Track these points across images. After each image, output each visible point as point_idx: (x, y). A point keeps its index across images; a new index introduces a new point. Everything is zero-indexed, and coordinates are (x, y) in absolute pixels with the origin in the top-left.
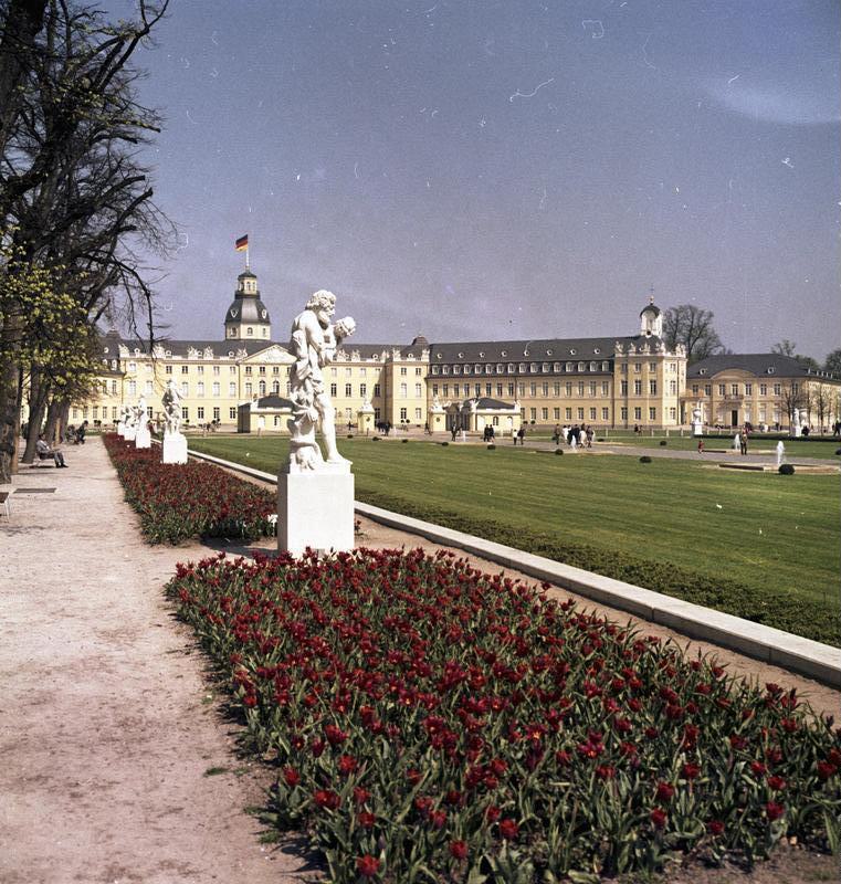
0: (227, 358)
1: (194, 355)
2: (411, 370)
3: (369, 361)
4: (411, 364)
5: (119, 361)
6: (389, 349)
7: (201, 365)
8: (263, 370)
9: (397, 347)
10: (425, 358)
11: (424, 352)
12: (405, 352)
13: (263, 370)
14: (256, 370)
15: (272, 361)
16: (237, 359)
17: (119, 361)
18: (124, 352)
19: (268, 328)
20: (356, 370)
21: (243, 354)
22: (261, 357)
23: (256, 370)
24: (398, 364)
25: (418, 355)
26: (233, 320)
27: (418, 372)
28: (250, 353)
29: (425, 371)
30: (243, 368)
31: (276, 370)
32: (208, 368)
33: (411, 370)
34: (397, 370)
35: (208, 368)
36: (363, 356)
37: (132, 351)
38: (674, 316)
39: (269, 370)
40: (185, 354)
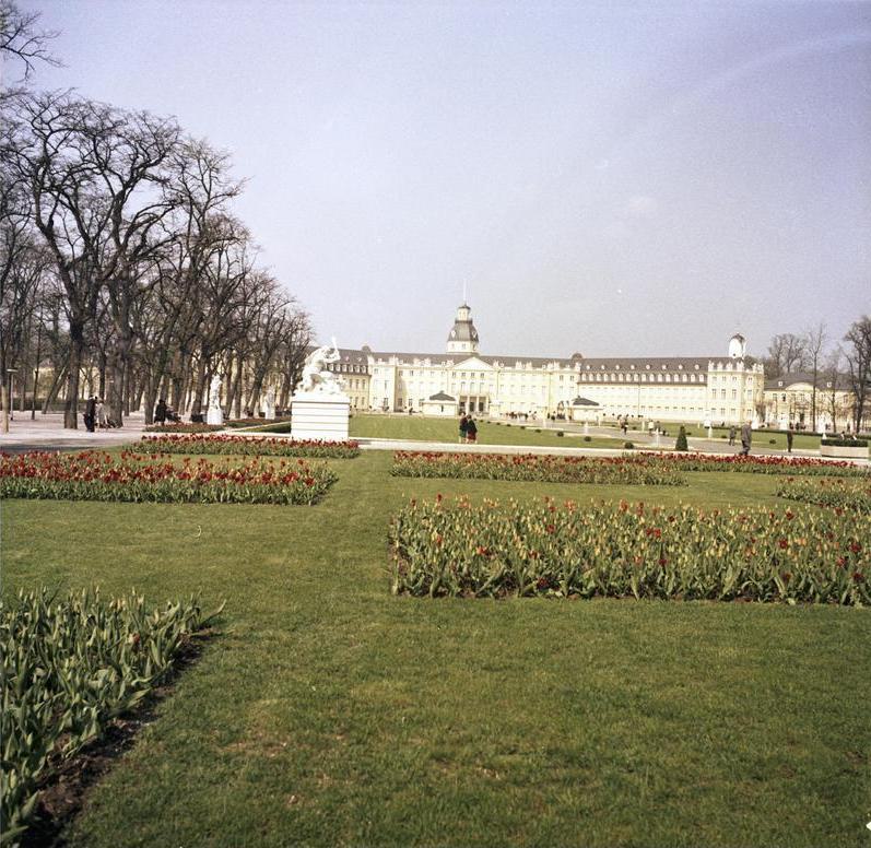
3: (538, 369)
4: (567, 373)
6: (551, 361)
8: (463, 374)
9: (557, 360)
10: (578, 368)
13: (463, 374)
14: (459, 374)
18: (371, 360)
20: (528, 377)
23: (459, 374)
25: (573, 366)
27: (572, 378)
28: (456, 362)
29: (577, 377)
30: (451, 372)
31: (473, 375)
32: (427, 373)
35: (427, 373)
37: (376, 360)
38: (779, 342)
39: (468, 374)
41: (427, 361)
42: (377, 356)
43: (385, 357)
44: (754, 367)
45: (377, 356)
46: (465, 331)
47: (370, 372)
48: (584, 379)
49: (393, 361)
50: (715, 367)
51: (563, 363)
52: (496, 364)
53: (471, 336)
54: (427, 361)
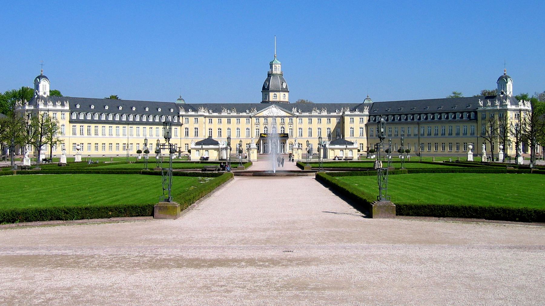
0: (244, 114)
2: (357, 119)
3: (332, 114)
5: (179, 117)
7: (320, 117)
10: (366, 112)
11: (366, 108)
12: (353, 110)
15: (271, 115)
16: (250, 114)
17: (179, 117)
18: (182, 113)
19: (287, 94)
22: (265, 113)
24: (347, 115)
25: (362, 110)
26: (266, 90)
27: (362, 121)
29: (366, 119)
33: (357, 119)
34: (347, 119)
36: (329, 111)
37: (187, 111)
39: (270, 120)
42: (187, 107)
43: (195, 108)
44: (521, 103)
45: (187, 107)
47: (181, 121)
50: (485, 105)
51: (354, 108)
52: (294, 110)
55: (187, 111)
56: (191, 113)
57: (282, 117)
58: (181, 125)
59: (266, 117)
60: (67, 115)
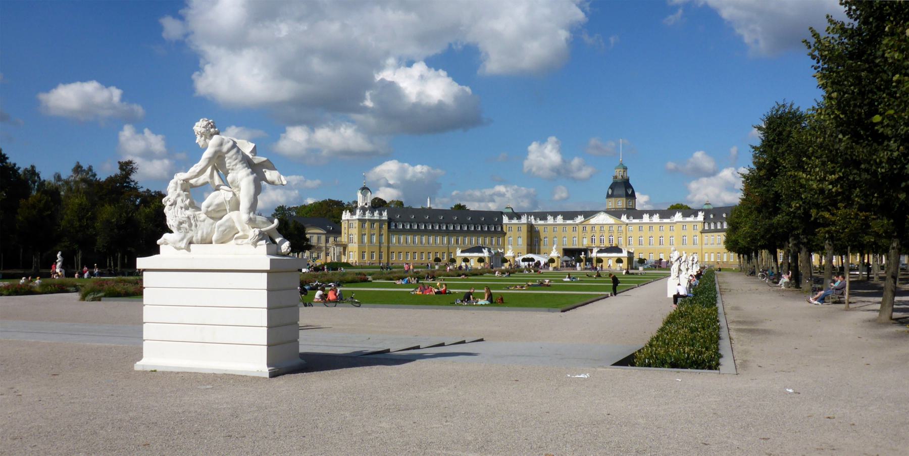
1: (550, 220)
2: (689, 227)
3: (665, 221)
18: (505, 220)
21: (580, 219)
25: (696, 216)
29: (700, 227)
30: (581, 227)
33: (689, 227)
37: (511, 218)
39: (597, 228)
40: (545, 219)
41: (560, 218)
43: (519, 216)
46: (622, 191)
48: (706, 228)
49: (524, 220)
52: (624, 218)
53: (627, 192)
54: (560, 218)
55: (511, 218)
56: (515, 221)
57: (611, 225)
58: (505, 234)
59: (593, 226)
60: (385, 227)
